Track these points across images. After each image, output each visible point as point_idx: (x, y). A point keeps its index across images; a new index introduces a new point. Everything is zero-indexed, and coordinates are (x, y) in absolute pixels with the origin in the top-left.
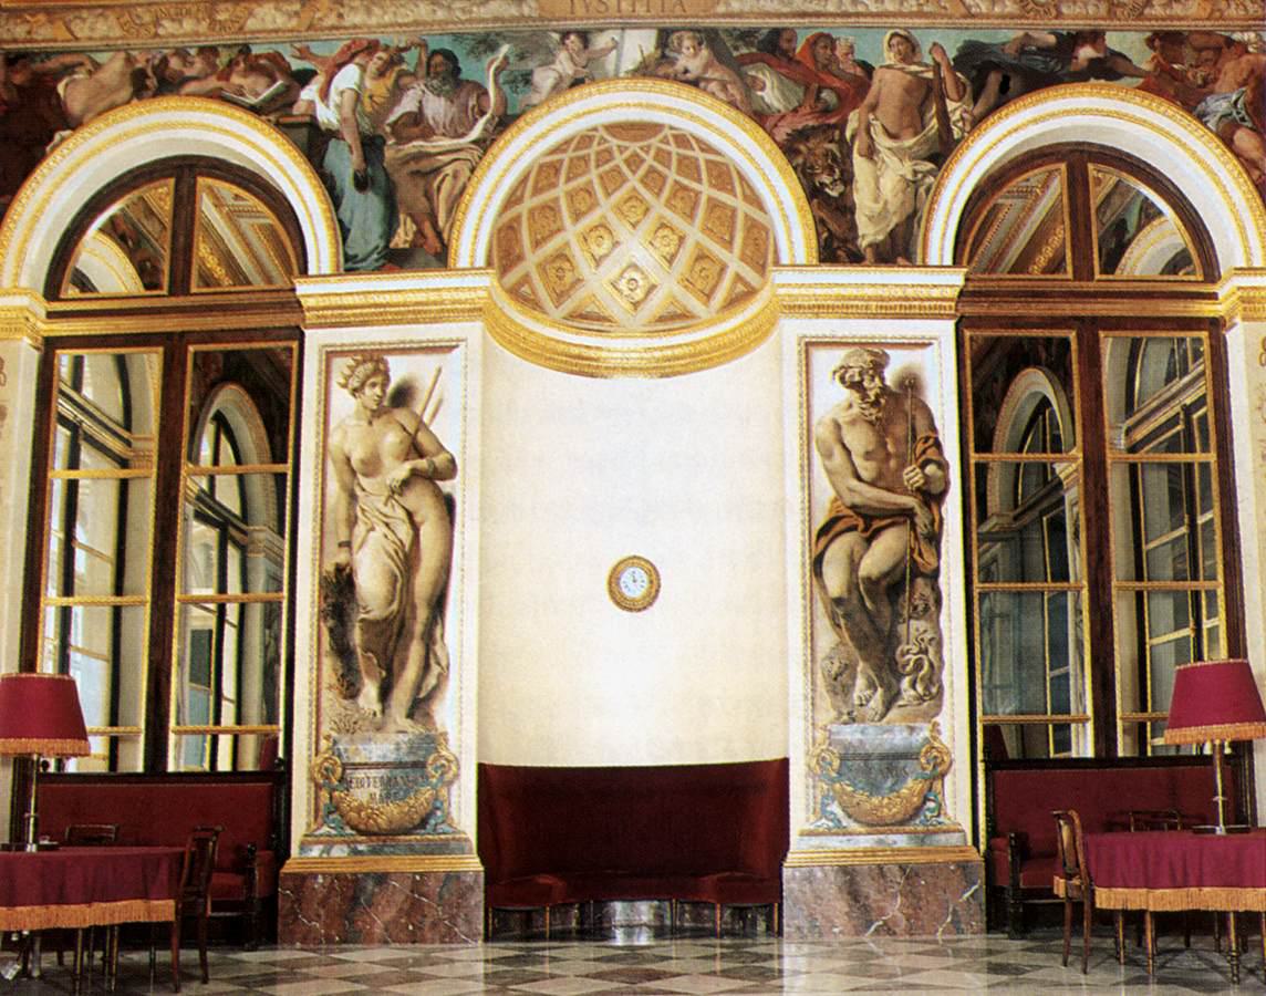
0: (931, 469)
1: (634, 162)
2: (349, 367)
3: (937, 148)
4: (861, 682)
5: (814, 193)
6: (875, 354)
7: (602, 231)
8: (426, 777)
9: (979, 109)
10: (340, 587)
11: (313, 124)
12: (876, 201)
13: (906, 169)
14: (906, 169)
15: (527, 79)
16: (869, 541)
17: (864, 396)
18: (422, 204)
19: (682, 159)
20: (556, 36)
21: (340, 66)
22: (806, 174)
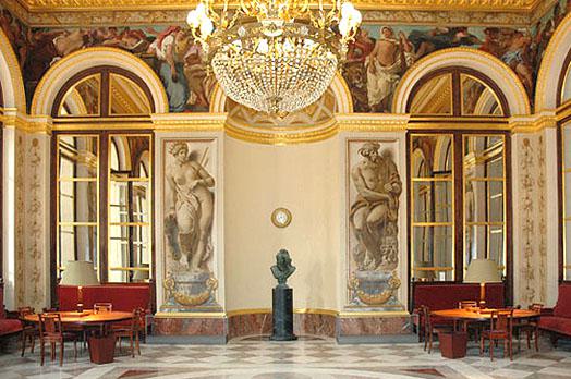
0: (395, 185)
4: (367, 257)
5: (351, 86)
8: (206, 287)
9: (417, 56)
10: (171, 223)
11: (155, 57)
13: (388, 78)
16: (371, 209)
17: (370, 158)
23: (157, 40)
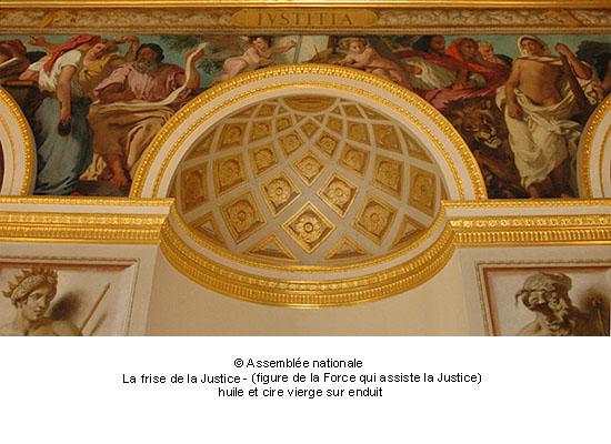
1: (309, 129)
2: (17, 278)
3: (578, 112)
5: (475, 146)
6: (553, 277)
7: (281, 184)
12: (533, 149)
13: (555, 126)
14: (555, 126)
15: (219, 65)
18: (116, 147)
19: (352, 126)
20: (246, 38)
21: (65, 51)
22: (465, 132)
23: (47, 58)
